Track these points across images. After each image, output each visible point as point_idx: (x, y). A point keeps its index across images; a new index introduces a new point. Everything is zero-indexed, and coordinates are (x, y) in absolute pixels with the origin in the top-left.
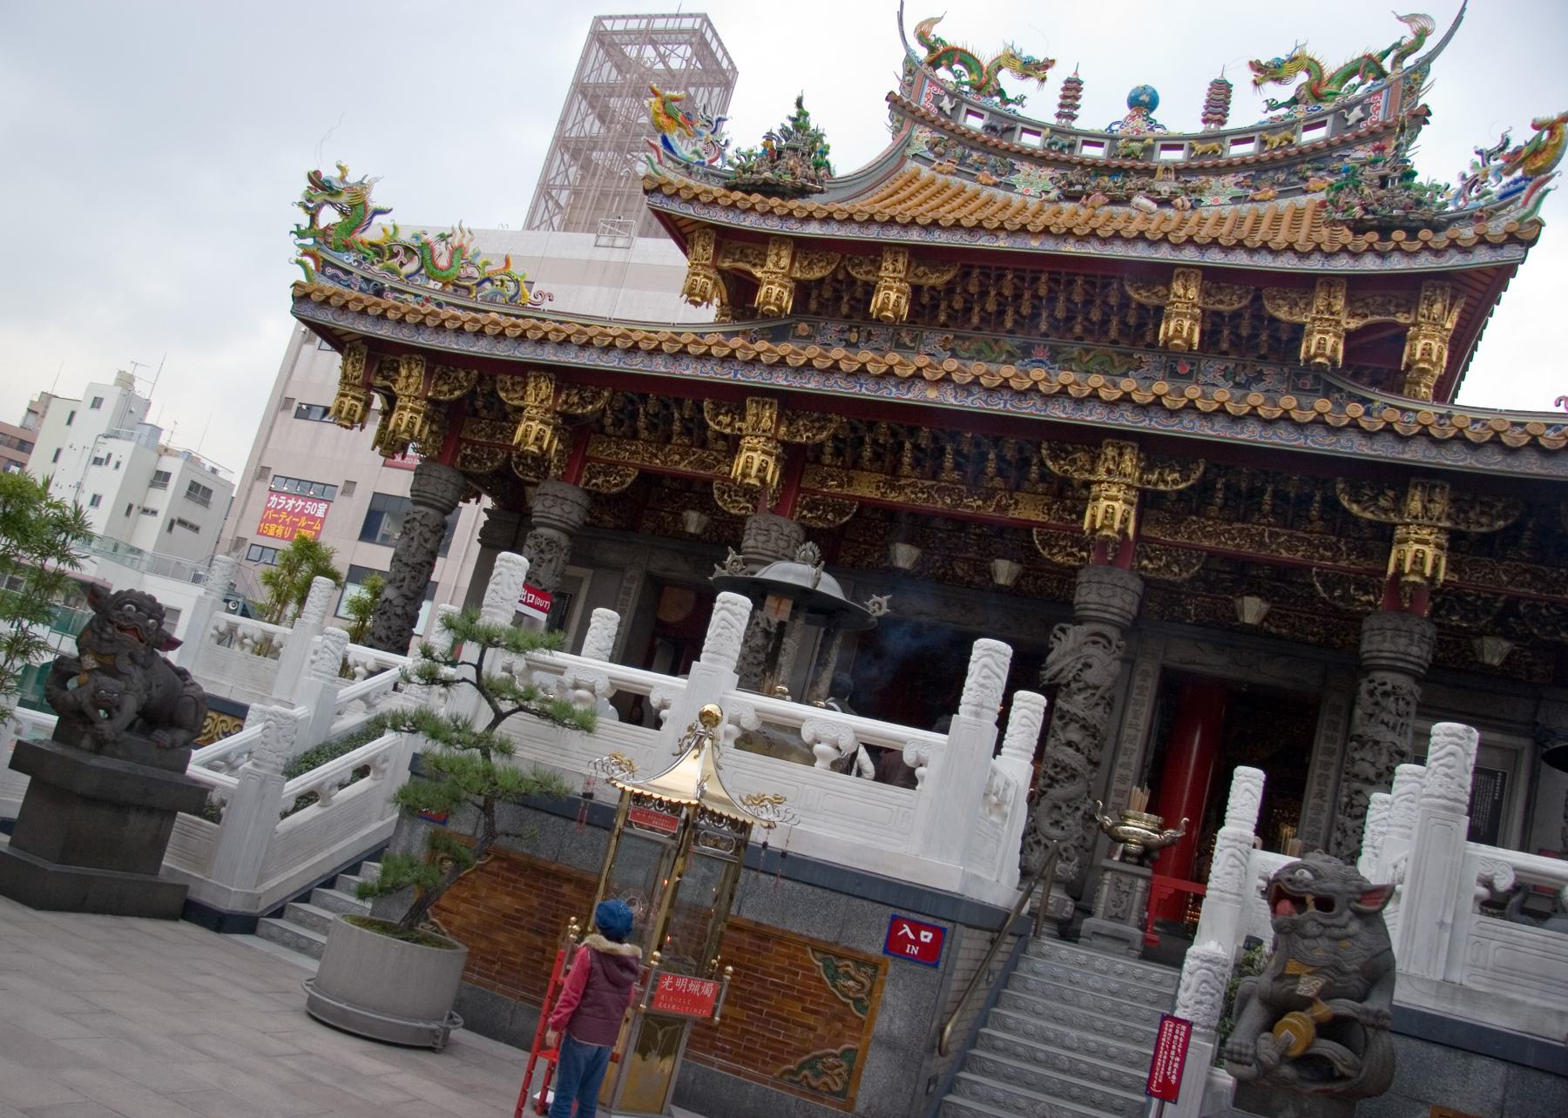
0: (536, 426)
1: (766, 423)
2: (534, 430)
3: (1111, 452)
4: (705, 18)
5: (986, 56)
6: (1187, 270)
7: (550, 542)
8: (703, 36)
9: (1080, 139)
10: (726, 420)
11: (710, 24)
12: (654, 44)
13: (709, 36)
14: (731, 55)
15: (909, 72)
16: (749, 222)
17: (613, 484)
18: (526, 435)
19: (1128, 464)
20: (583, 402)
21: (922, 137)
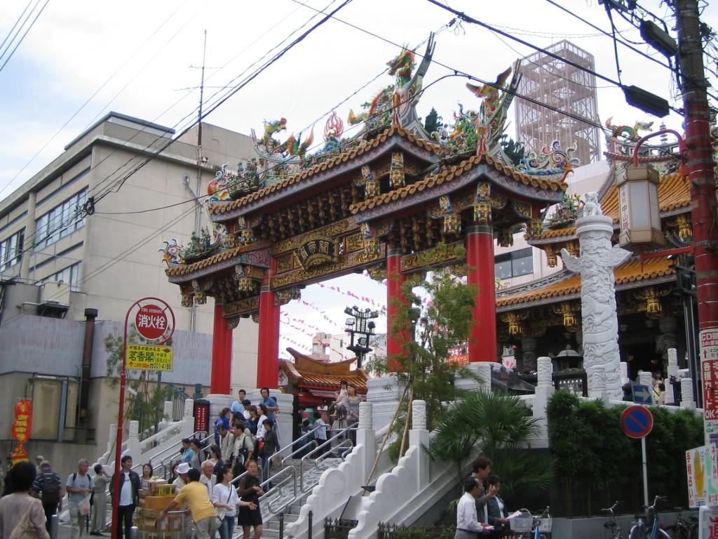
0: (513, 327)
1: (567, 309)
2: (513, 328)
3: (647, 291)
4: (565, 42)
5: (632, 125)
6: (680, 215)
7: (529, 355)
8: (568, 50)
9: (670, 147)
10: (558, 310)
11: (569, 43)
12: (546, 63)
13: (571, 48)
14: (586, 50)
15: (608, 142)
16: (557, 240)
17: (540, 333)
18: (511, 330)
19: (652, 293)
20: (524, 316)
21: (619, 164)
